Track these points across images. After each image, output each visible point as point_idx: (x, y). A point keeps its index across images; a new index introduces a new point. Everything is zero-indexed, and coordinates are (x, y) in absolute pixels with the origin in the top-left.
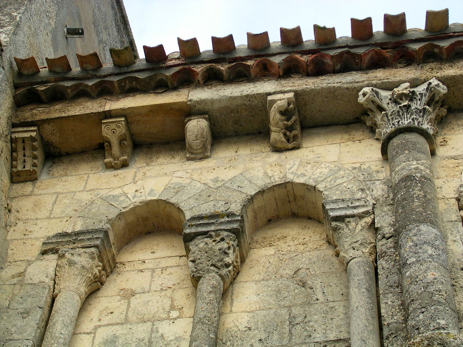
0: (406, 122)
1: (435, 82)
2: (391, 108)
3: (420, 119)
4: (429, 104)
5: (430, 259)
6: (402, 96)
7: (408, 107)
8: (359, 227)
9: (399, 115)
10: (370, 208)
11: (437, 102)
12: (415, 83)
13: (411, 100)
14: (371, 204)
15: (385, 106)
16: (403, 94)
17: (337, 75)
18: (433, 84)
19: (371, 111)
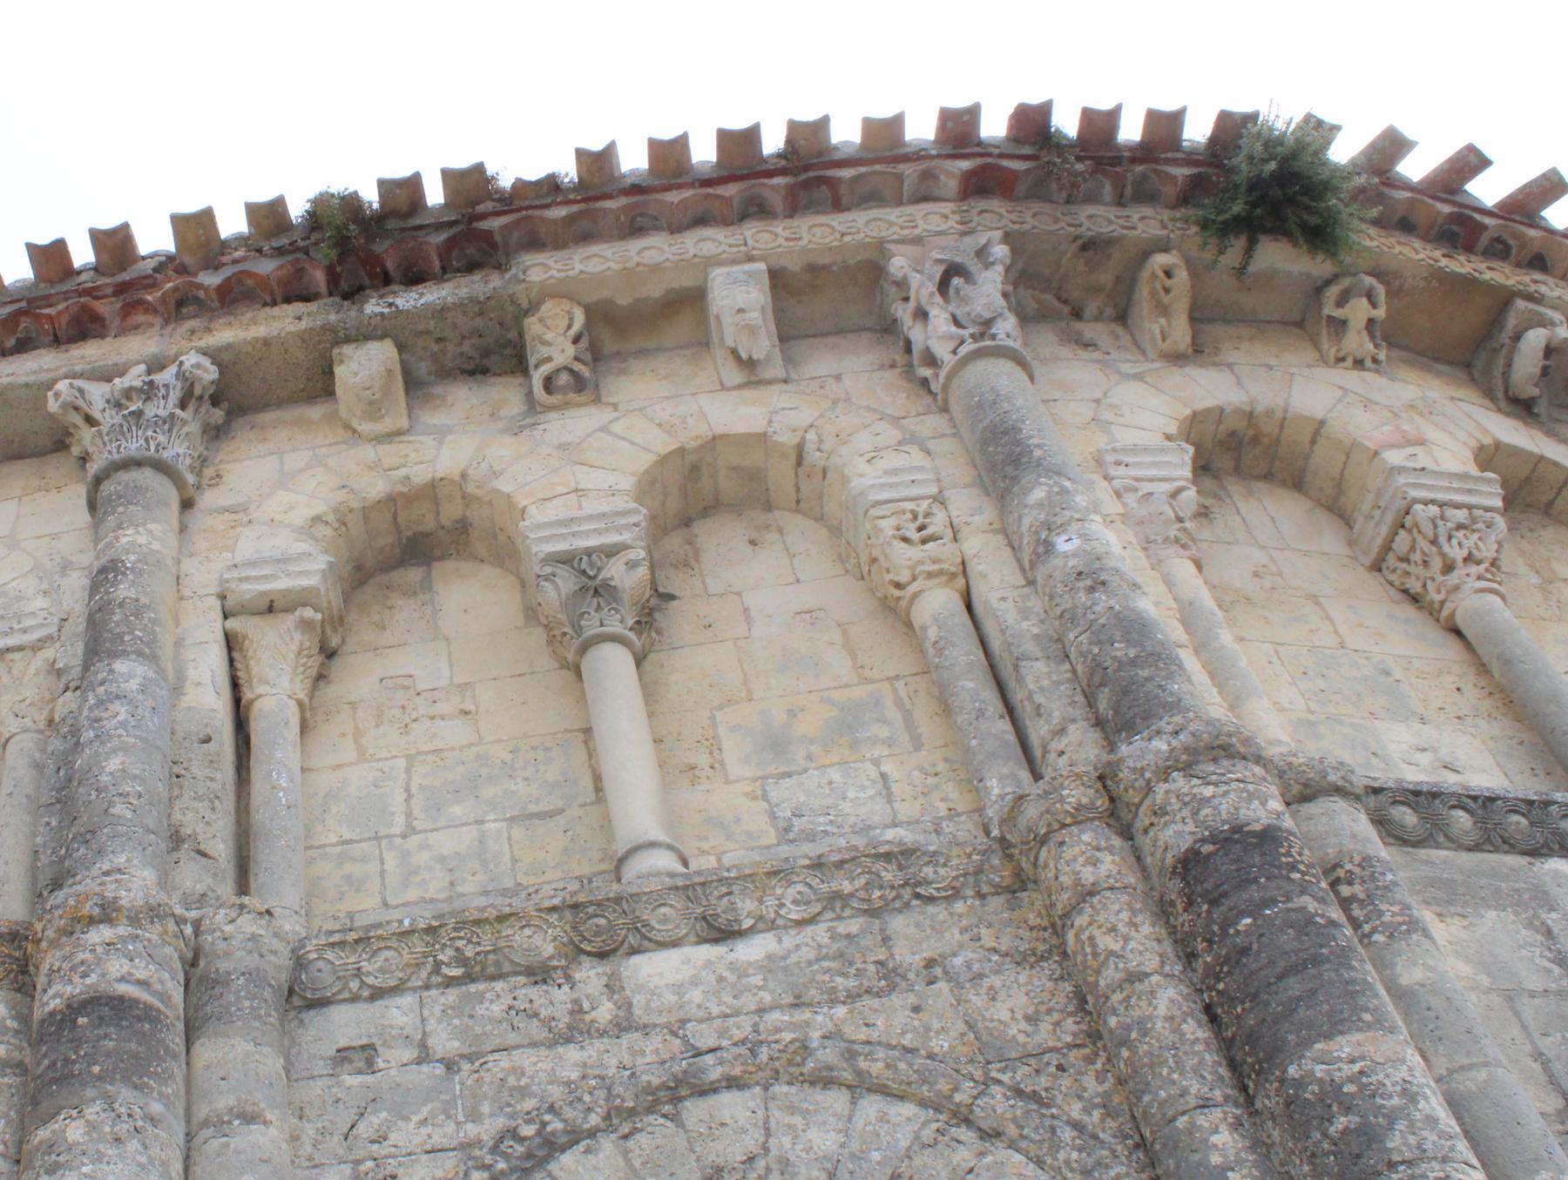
0: (133, 446)
1: (190, 359)
2: (109, 418)
3: (161, 438)
6: (128, 393)
7: (138, 414)
8: (32, 670)
9: (123, 434)
10: (53, 630)
11: (201, 398)
12: (156, 365)
13: (148, 399)
14: (56, 620)
15: (97, 415)
16: (131, 389)
17: (10, 359)
18: (187, 365)
19: (75, 426)
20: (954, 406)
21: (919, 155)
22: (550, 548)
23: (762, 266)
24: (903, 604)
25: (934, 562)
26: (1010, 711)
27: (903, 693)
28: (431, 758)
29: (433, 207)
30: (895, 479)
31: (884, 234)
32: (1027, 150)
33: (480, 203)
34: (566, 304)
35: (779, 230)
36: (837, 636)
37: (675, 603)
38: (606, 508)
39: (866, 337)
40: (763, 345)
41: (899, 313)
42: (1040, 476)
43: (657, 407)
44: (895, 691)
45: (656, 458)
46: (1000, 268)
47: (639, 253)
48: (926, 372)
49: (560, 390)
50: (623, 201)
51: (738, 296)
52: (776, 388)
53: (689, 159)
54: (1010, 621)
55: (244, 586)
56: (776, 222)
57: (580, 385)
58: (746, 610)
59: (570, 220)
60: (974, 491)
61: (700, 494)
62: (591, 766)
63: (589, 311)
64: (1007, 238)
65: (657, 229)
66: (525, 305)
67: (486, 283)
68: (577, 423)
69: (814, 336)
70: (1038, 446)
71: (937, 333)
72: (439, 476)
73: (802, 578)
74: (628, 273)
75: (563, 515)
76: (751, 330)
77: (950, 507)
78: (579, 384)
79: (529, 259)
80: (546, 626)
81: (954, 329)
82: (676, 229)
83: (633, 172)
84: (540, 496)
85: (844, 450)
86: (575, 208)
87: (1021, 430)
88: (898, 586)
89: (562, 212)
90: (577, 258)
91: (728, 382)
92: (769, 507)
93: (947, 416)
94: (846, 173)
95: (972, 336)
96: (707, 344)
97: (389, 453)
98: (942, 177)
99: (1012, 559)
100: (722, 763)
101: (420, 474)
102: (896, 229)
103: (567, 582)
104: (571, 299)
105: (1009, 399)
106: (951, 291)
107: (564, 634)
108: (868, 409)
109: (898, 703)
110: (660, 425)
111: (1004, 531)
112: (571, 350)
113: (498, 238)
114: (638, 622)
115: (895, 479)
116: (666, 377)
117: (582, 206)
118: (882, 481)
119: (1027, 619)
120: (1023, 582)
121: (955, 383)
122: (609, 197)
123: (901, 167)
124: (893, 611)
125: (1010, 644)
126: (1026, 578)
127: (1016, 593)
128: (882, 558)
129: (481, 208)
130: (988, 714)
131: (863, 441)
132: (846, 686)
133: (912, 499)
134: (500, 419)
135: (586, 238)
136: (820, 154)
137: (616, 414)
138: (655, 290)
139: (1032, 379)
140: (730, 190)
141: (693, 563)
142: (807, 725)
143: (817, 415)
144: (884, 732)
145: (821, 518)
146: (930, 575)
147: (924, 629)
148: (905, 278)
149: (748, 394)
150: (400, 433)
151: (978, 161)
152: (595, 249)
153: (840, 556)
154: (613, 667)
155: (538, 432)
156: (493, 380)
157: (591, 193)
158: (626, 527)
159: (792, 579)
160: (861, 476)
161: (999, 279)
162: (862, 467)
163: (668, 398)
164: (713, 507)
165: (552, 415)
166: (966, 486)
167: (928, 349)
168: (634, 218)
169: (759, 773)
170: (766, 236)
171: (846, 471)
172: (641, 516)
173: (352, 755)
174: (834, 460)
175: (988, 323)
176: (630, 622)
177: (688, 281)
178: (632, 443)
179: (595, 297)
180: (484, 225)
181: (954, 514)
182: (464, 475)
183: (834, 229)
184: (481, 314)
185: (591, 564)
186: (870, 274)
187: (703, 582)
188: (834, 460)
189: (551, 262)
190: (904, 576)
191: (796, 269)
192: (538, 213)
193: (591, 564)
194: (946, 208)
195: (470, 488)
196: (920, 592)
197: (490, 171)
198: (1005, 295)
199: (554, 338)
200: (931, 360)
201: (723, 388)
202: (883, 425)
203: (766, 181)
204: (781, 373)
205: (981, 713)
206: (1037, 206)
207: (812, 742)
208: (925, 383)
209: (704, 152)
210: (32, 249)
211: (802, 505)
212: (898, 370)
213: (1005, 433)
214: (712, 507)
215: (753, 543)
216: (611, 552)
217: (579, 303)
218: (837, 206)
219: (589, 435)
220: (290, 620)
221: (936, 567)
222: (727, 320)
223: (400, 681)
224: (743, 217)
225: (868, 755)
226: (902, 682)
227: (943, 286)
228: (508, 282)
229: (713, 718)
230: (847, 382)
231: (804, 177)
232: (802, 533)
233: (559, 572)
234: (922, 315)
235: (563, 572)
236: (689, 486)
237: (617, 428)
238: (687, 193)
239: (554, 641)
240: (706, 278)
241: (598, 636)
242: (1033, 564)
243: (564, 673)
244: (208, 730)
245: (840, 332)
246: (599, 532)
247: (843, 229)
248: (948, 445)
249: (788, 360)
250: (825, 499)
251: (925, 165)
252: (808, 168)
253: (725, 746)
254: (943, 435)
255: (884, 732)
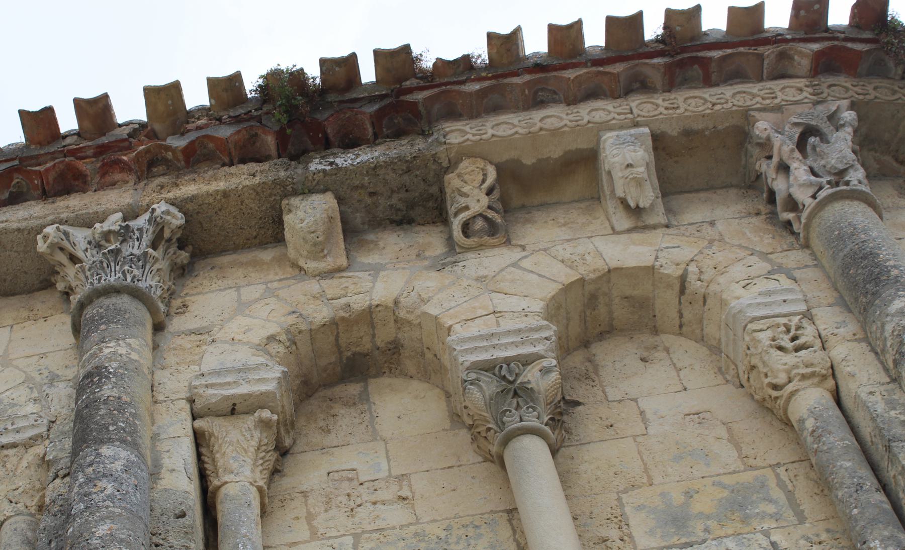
0: (112, 279)
1: (161, 208)
2: (90, 257)
3: (136, 272)
4: (154, 246)
5: (108, 503)
6: (107, 235)
7: (116, 252)
8: (24, 464)
9: (103, 269)
10: (43, 429)
11: (169, 240)
12: (131, 214)
14: (45, 421)
15: (80, 254)
16: (110, 232)
18: (158, 212)
19: (61, 264)
20: (815, 242)
21: (777, 38)
22: (473, 358)
23: (646, 130)
24: (781, 402)
25: (807, 367)
26: (884, 487)
27: (784, 476)
28: (375, 535)
29: (366, 84)
30: (769, 299)
31: (749, 103)
32: (868, 35)
33: (407, 80)
34: (481, 163)
35: (660, 101)
36: (723, 432)
37: (580, 408)
38: (522, 326)
39: (733, 192)
40: (647, 196)
41: (764, 168)
42: (898, 290)
43: (559, 248)
44: (777, 476)
45: (561, 287)
46: (849, 129)
47: (541, 120)
48: (790, 216)
49: (475, 234)
50: (527, 77)
51: (626, 155)
52: (660, 232)
53: (583, 42)
54: (879, 411)
55: (211, 391)
56: (656, 96)
57: (494, 229)
58: (642, 413)
59: (483, 93)
60: (837, 309)
61: (597, 318)
62: (515, 540)
63: (499, 168)
64: (853, 106)
65: (556, 102)
66: (445, 164)
67: (412, 145)
68: (494, 260)
69: (689, 192)
70: (895, 267)
71: (799, 182)
72: (375, 303)
73: (688, 387)
74: (533, 136)
75: (485, 331)
76: (639, 183)
77: (817, 322)
78: (492, 229)
79: (448, 126)
80: (471, 427)
81: (813, 178)
82: (572, 101)
83: (535, 55)
84: (464, 317)
85: (721, 279)
86: (487, 84)
87: (878, 255)
88: (775, 387)
89: (477, 87)
90: (489, 125)
91: (618, 228)
92: (656, 331)
93: (808, 252)
94: (716, 54)
95: (829, 182)
96: (599, 199)
97: (332, 286)
98: (796, 57)
99: (876, 362)
100: (630, 536)
101: (359, 302)
102: (759, 99)
103: (490, 385)
104: (484, 159)
105: (865, 231)
106: (809, 148)
107: (489, 429)
108: (740, 246)
109: (781, 485)
110: (563, 262)
111: (866, 340)
112: (485, 200)
113: (421, 108)
114: (552, 419)
115: (769, 299)
116: (564, 225)
117: (493, 82)
118: (758, 300)
119: (895, 409)
120: (888, 380)
121: (816, 222)
122: (516, 74)
123: (761, 49)
124: (770, 410)
125: (881, 430)
126: (890, 376)
127: (882, 388)
128: (760, 365)
129: (407, 84)
130: (865, 487)
131: (738, 271)
132: (734, 472)
133: (785, 316)
134: (426, 259)
135: (496, 109)
136: (693, 39)
137: (524, 254)
138: (555, 152)
139: (881, 217)
140: (617, 68)
141: (593, 376)
142: (702, 504)
143: (696, 252)
144: (771, 509)
145: (701, 339)
146: (804, 377)
147: (802, 421)
148: (768, 139)
149: (635, 236)
150: (340, 270)
151: (827, 44)
152: (503, 118)
153: (720, 369)
154: (532, 456)
155: (458, 269)
156: (418, 228)
157: (500, 72)
158: (539, 340)
159: (680, 388)
160: (738, 298)
161: (849, 138)
162: (738, 290)
163: (568, 241)
164: (609, 332)
165: (470, 255)
166: (830, 305)
167: (790, 196)
168: (536, 93)
169: (663, 544)
170: (649, 106)
171: (724, 296)
172: (551, 331)
173: (306, 535)
174: (713, 288)
175: (842, 173)
176: (546, 419)
177: (583, 143)
178: (540, 275)
179: (505, 157)
180: (409, 98)
181: (821, 327)
182: (396, 302)
183: (706, 101)
184: (408, 171)
185: (510, 371)
186: (738, 137)
187: (604, 392)
188: (713, 288)
189: (467, 128)
190: (782, 378)
191: (675, 133)
192: (456, 87)
193: (510, 371)
194: (801, 83)
195: (402, 314)
196: (797, 391)
197: (416, 51)
198: (854, 152)
199: (470, 190)
200: (793, 205)
201: (615, 232)
202: (754, 259)
203: (647, 61)
204: (663, 220)
205: (859, 487)
206: (877, 82)
207: (708, 517)
208: (789, 223)
209: (595, 37)
210: (24, 115)
211: (684, 329)
212: (763, 217)
213: (865, 257)
214: (609, 331)
215: (643, 360)
216: (526, 361)
217: (491, 163)
218: (708, 82)
219: (502, 270)
220: (250, 421)
221: (809, 370)
222: (618, 174)
223: (344, 474)
224: (628, 92)
225: (759, 528)
226: (783, 469)
227: (801, 145)
228: (432, 144)
229: (619, 499)
230: (720, 226)
231: (679, 57)
232: (685, 351)
233: (483, 378)
234: (784, 168)
235: (485, 378)
236: (588, 313)
237: (525, 264)
238: (582, 71)
239: (477, 435)
240: (598, 143)
241: (519, 429)
242: (896, 363)
243: (487, 465)
244: (183, 507)
245: (710, 188)
246: (515, 344)
247: (714, 99)
248: (811, 274)
249: (669, 211)
250: (705, 322)
251: (783, 47)
252: (684, 50)
253: (632, 522)
254: (806, 266)
255: (771, 509)
